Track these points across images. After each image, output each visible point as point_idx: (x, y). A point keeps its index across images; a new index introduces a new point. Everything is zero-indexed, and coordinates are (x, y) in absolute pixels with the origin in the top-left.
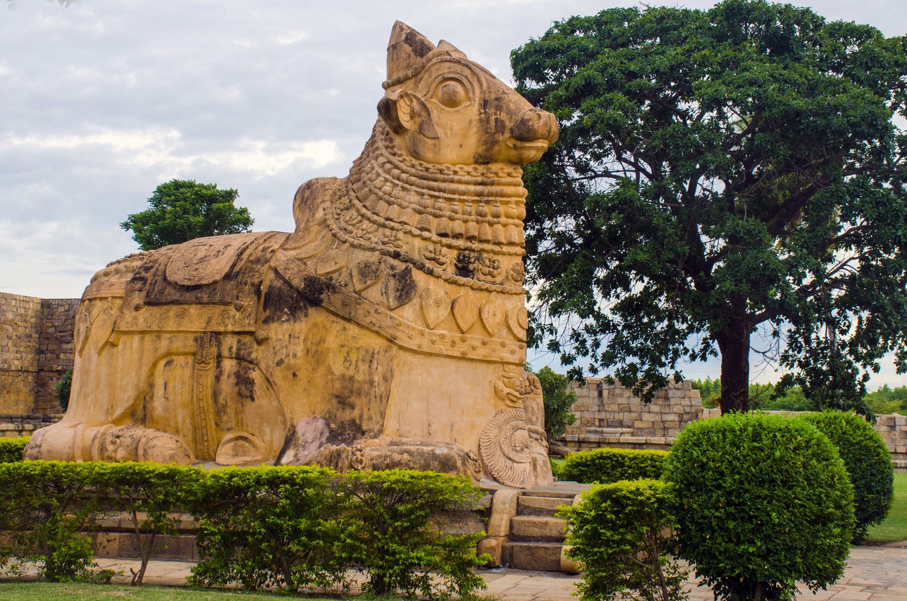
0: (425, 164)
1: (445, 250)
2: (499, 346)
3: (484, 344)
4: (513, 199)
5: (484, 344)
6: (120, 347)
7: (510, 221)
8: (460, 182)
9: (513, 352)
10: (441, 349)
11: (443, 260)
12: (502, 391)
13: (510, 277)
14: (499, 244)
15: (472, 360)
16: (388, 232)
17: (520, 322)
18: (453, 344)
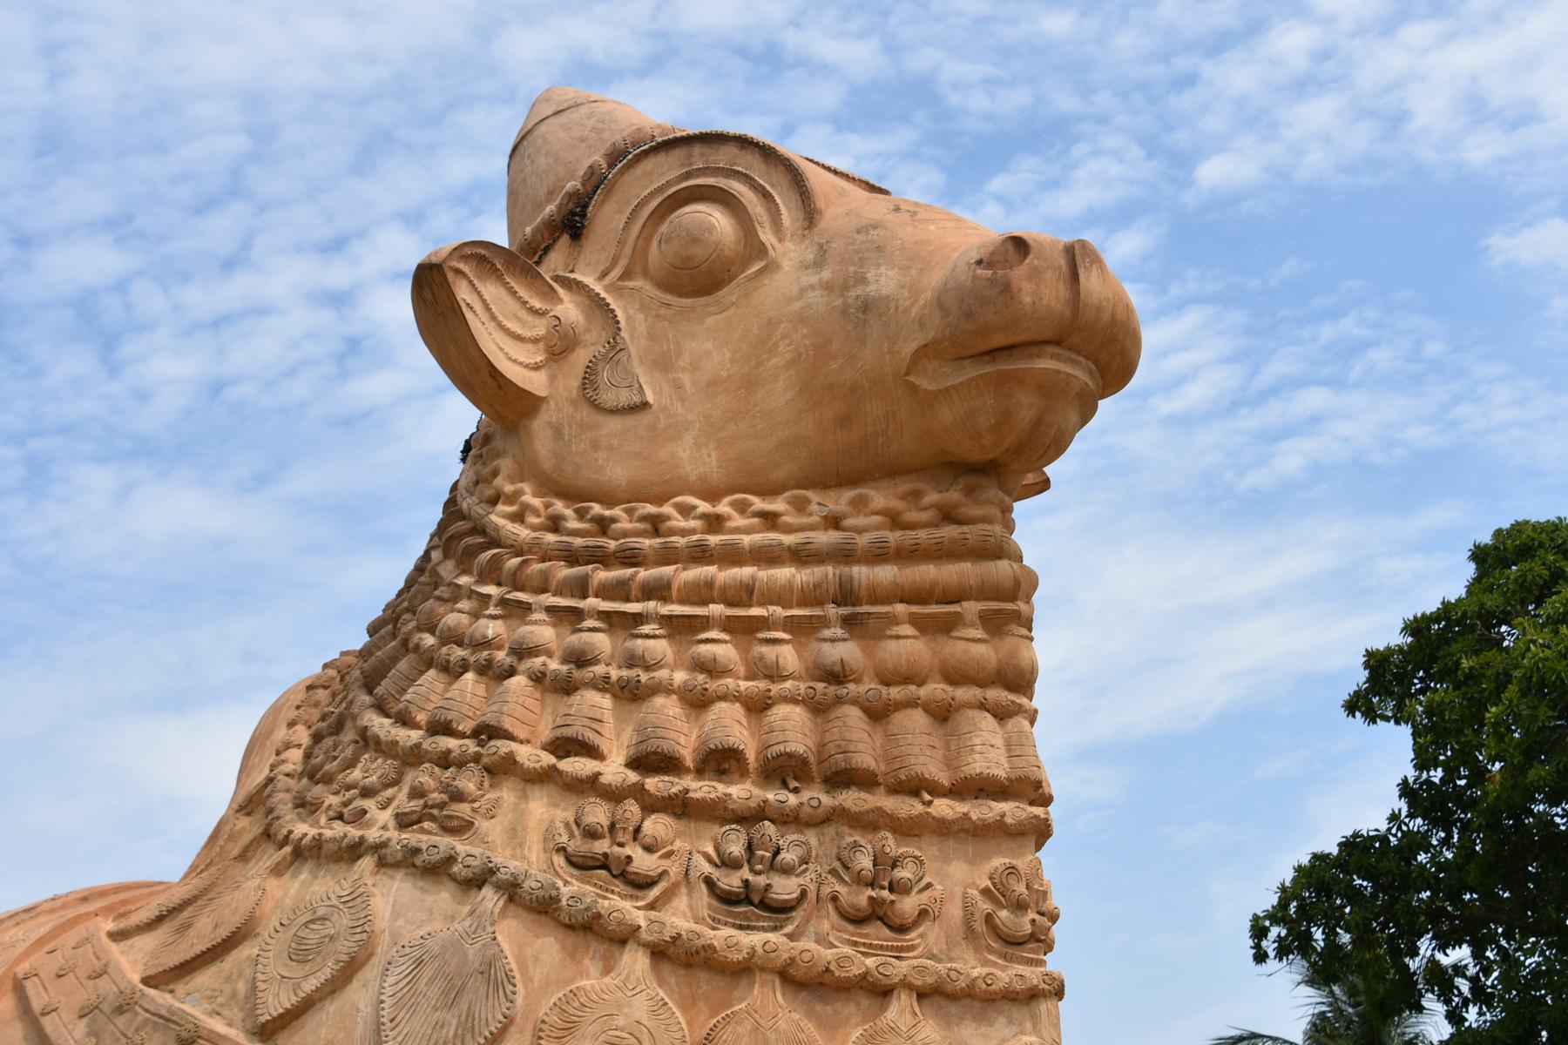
0: (597, 509)
1: (657, 825)
4: (971, 608)
7: (964, 693)
8: (732, 556)
11: (643, 862)
13: (980, 926)
14: (915, 787)
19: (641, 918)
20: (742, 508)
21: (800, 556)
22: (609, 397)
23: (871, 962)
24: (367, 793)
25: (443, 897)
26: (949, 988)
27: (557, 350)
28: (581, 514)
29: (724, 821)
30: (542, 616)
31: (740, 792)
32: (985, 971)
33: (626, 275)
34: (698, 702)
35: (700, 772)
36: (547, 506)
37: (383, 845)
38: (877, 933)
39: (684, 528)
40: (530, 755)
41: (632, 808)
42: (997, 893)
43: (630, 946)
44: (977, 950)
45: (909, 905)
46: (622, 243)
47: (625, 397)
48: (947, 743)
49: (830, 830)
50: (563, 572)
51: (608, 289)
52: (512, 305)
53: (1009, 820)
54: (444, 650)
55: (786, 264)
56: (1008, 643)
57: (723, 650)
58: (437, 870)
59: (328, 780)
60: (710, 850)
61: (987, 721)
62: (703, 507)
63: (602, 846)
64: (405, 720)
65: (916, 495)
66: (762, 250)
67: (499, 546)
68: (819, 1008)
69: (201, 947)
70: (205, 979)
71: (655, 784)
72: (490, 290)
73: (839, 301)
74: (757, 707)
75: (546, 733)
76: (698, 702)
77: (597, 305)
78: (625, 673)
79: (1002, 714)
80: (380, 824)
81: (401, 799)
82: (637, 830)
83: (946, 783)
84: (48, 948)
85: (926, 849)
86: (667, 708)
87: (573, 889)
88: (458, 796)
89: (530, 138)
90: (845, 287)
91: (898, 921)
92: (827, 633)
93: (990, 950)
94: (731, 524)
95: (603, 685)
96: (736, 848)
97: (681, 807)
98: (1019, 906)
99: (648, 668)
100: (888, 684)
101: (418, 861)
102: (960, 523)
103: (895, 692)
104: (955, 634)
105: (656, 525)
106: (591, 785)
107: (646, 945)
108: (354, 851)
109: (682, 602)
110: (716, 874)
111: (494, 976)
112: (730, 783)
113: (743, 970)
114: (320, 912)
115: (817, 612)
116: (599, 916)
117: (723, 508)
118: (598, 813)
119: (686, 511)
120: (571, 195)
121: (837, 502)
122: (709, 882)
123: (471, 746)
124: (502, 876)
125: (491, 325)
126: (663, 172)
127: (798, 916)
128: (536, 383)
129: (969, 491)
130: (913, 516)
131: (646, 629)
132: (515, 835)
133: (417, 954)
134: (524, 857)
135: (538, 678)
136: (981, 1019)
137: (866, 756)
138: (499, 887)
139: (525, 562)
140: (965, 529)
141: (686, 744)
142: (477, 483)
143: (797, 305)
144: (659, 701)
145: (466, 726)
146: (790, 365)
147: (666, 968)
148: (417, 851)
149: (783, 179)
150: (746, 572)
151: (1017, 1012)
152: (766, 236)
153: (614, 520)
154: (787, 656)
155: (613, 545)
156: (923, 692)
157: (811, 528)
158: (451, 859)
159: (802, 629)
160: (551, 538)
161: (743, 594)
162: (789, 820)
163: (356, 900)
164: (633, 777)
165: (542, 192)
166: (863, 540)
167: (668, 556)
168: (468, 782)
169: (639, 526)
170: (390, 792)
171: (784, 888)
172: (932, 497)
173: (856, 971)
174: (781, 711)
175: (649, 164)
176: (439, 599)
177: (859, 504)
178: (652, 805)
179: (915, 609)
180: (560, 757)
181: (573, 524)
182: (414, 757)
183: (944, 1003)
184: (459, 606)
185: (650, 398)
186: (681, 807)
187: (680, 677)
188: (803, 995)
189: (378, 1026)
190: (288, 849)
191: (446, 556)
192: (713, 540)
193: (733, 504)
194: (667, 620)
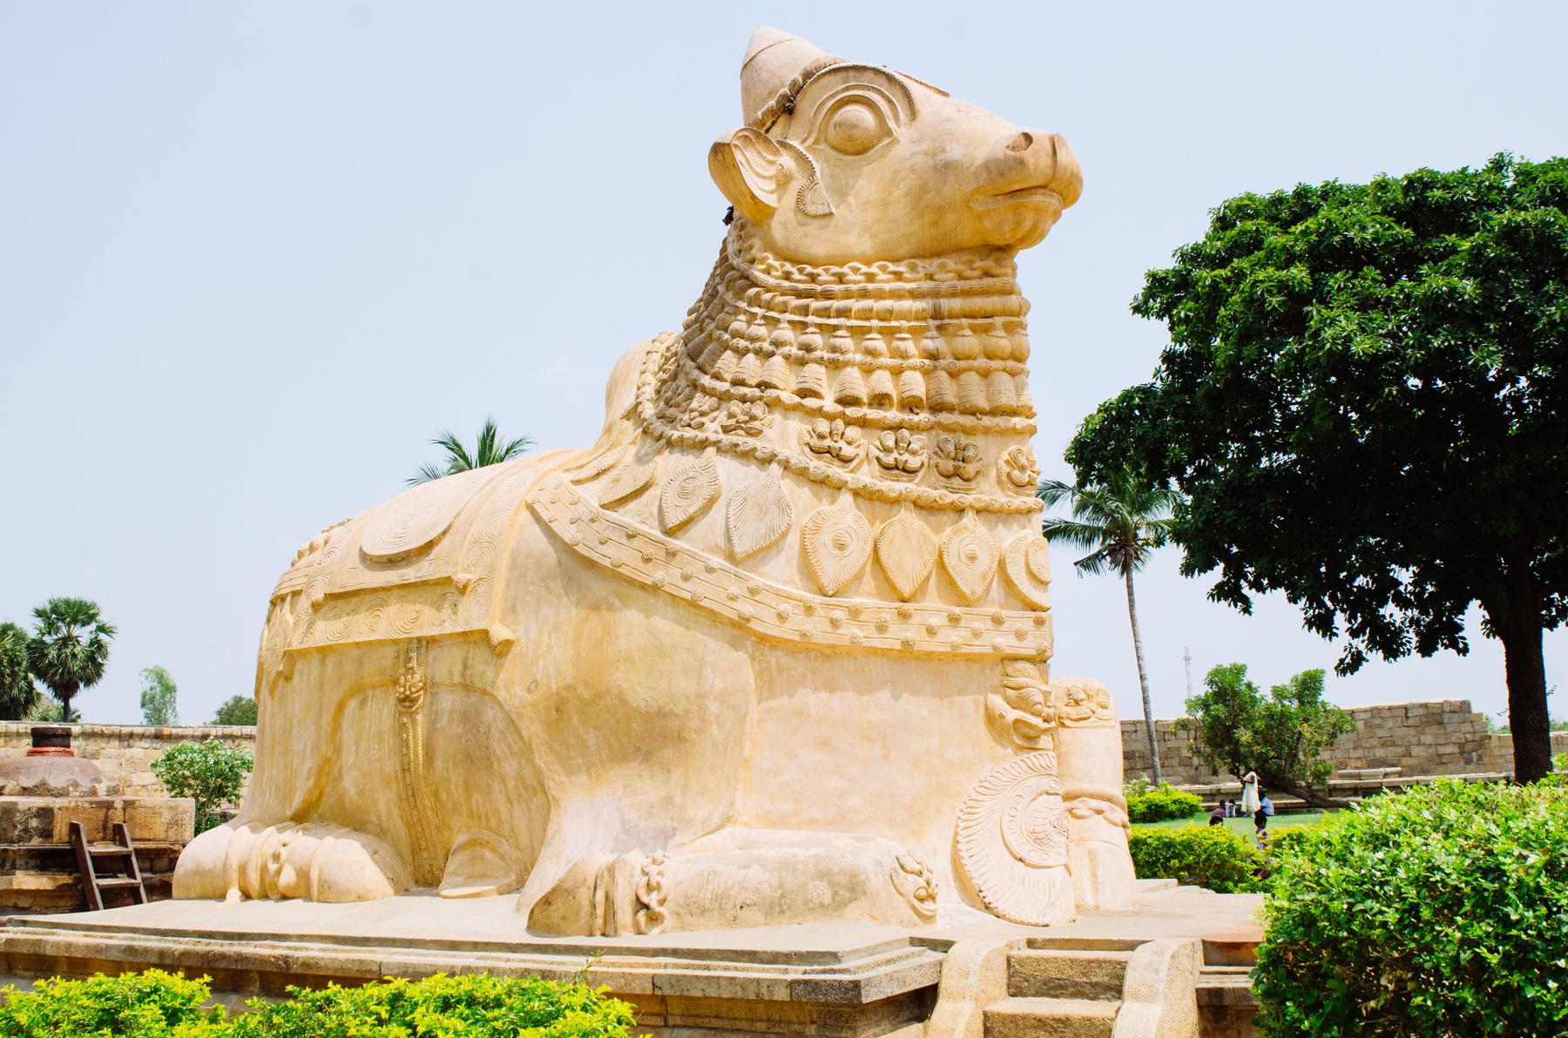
0: (809, 269)
1: (853, 432)
2: (989, 624)
3: (954, 620)
4: (999, 320)
5: (954, 620)
6: (296, 679)
7: (995, 364)
8: (880, 295)
9: (1020, 635)
10: (854, 637)
11: (847, 451)
12: (1002, 716)
13: (1004, 478)
14: (974, 412)
15: (929, 656)
16: (736, 407)
17: (1034, 568)
18: (881, 628)
19: (847, 477)
20: (883, 269)
21: (915, 295)
22: (812, 209)
23: (955, 497)
24: (703, 414)
25: (753, 469)
26: (991, 508)
27: (782, 182)
28: (801, 271)
29: (884, 429)
30: (786, 325)
31: (893, 415)
32: (1007, 499)
33: (816, 142)
34: (868, 370)
35: (870, 405)
36: (782, 266)
37: (719, 442)
38: (957, 482)
39: (856, 281)
40: (788, 397)
41: (839, 423)
42: (1013, 462)
43: (843, 490)
44: (1003, 490)
45: (970, 469)
46: (812, 124)
47: (821, 210)
48: (988, 391)
49: (933, 433)
50: (794, 302)
51: (806, 148)
52: (760, 161)
53: (1018, 427)
54: (735, 341)
55: (902, 139)
56: (1017, 337)
57: (879, 343)
58: (747, 455)
59: (677, 405)
60: (878, 443)
61: (1005, 377)
62: (864, 269)
63: (827, 442)
64: (717, 377)
65: (971, 262)
66: (889, 133)
67: (756, 285)
68: (931, 518)
69: (629, 491)
70: (633, 505)
71: (851, 412)
72: (751, 155)
73: (931, 162)
74: (897, 372)
75: (794, 386)
76: (868, 370)
77: (801, 158)
78: (832, 356)
79: (1013, 374)
80: (712, 430)
81: (722, 416)
82: (843, 434)
83: (988, 409)
84: (538, 487)
85: (979, 441)
86: (853, 374)
87: (817, 465)
88: (753, 418)
89: (755, 60)
90: (935, 154)
91: (966, 477)
92: (929, 334)
93: (1009, 489)
94: (879, 278)
95: (820, 361)
96: (890, 443)
97: (863, 423)
98: (1023, 469)
99: (842, 353)
100: (958, 359)
101: (739, 450)
102: (993, 276)
103: (962, 364)
104: (994, 333)
105: (841, 279)
106: (819, 412)
107: (851, 490)
108: (703, 445)
109: (856, 318)
110: (881, 455)
111: (783, 507)
112: (885, 410)
113: (896, 502)
114: (691, 474)
115: (923, 324)
116: (829, 476)
117: (874, 269)
118: (823, 426)
119: (855, 270)
120: (784, 96)
121: (930, 265)
122: (878, 459)
123: (757, 392)
124: (781, 457)
125: (750, 171)
126: (833, 88)
127: (920, 474)
128: (770, 200)
129: (997, 261)
130: (968, 273)
131: (840, 333)
132: (783, 436)
133: (744, 495)
134: (789, 448)
135: (787, 357)
136: (1005, 522)
137: (950, 397)
138: (779, 463)
139: (774, 296)
140: (995, 279)
141: (863, 393)
142: (740, 251)
143: (910, 162)
144: (849, 369)
145: (753, 382)
146: (908, 193)
147: (860, 500)
148: (736, 445)
149: (899, 93)
150: (888, 304)
151: (1022, 519)
152: (891, 124)
153: (819, 275)
154: (909, 346)
155: (819, 288)
156: (976, 364)
157: (919, 280)
158: (755, 449)
159: (917, 333)
160: (786, 284)
161: (887, 315)
162: (915, 428)
163: (707, 468)
164: (839, 408)
165: (766, 93)
166: (944, 287)
167: (848, 295)
168: (758, 409)
169: (832, 278)
170: (715, 414)
171: (914, 462)
172: (978, 264)
173: (948, 501)
174: (907, 374)
175: (825, 80)
176: (727, 313)
177: (943, 267)
178: (849, 422)
179: (971, 321)
180: (803, 398)
181: (797, 276)
182: (724, 397)
183: (989, 515)
184: (739, 317)
185: (834, 211)
186: (863, 423)
187: (859, 357)
188: (924, 512)
189: (728, 530)
190: (663, 441)
191: (727, 289)
192: (871, 286)
193: (879, 267)
194: (850, 328)
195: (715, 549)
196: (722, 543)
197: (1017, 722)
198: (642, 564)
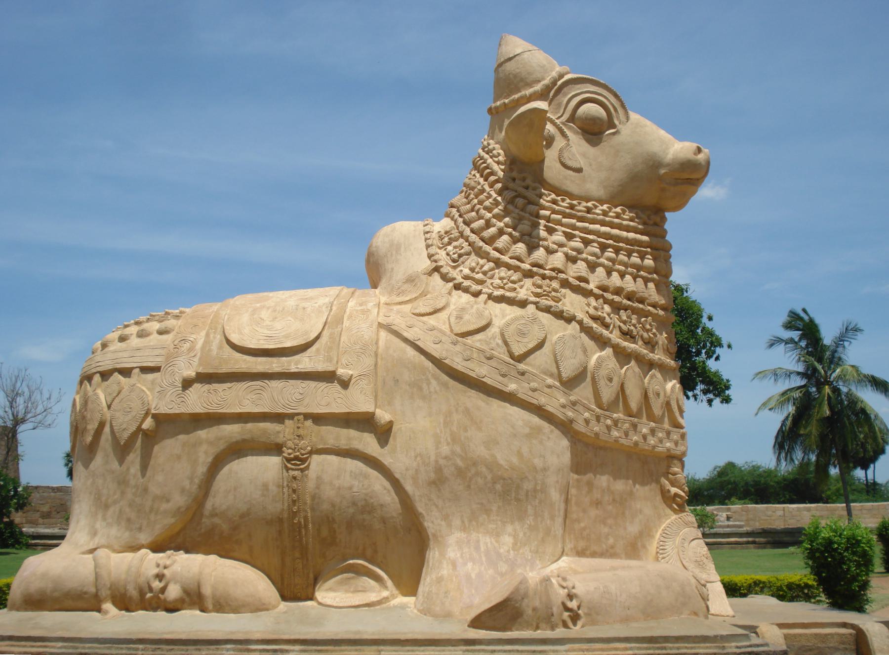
8: (612, 225)
30: (561, 233)
33: (568, 121)
37: (538, 302)
66: (613, 126)
122: (620, 327)
124: (578, 318)
135: (566, 255)
164: (601, 292)
195: (551, 375)
196: (555, 370)
197: (676, 495)
198: (501, 378)
